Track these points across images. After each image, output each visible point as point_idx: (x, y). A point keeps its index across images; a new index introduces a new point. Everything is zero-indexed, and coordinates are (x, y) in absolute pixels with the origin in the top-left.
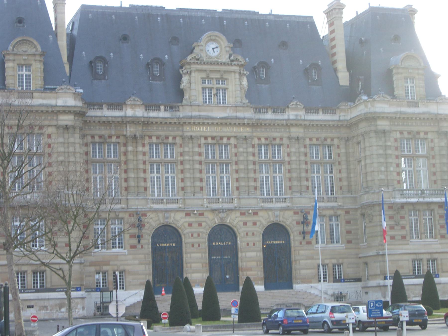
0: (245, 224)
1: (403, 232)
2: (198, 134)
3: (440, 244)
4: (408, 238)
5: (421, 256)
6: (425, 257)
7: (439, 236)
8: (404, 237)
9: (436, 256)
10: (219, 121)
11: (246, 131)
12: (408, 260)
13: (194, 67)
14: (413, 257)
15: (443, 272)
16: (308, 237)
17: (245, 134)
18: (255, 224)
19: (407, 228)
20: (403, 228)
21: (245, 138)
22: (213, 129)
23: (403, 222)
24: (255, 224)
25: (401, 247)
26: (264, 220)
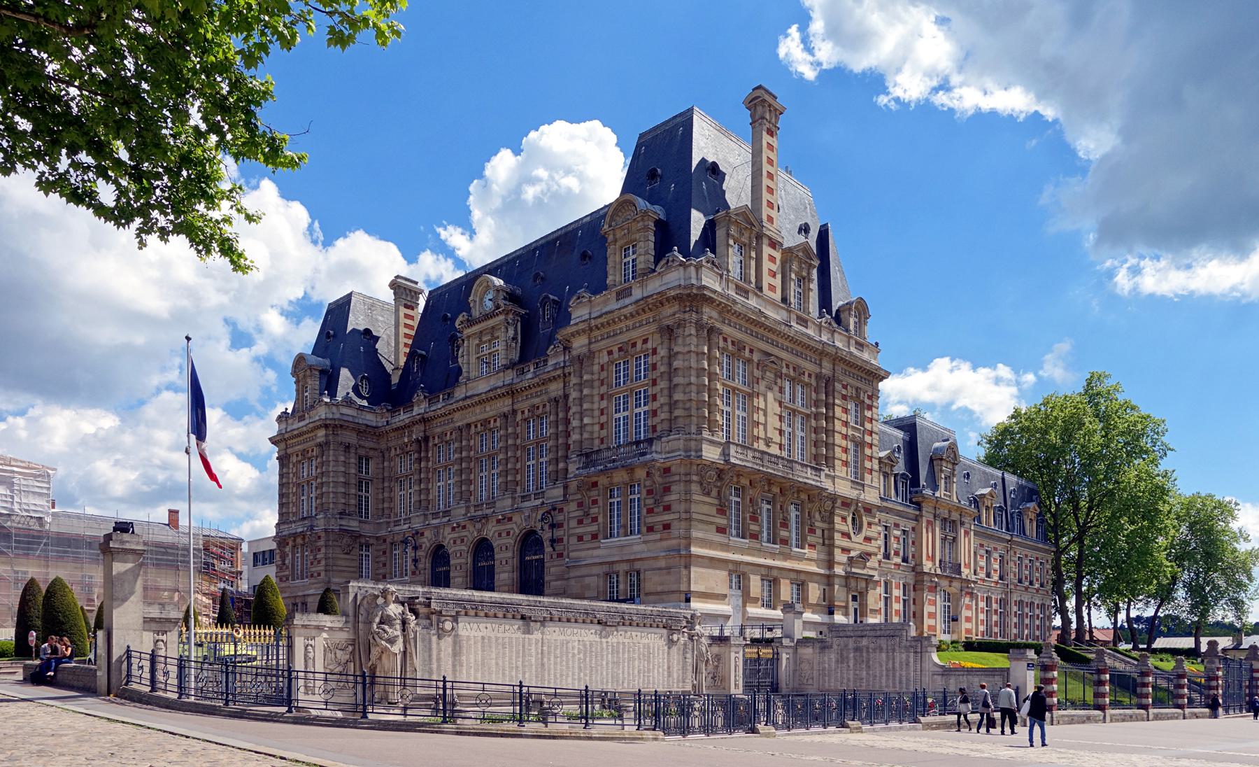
0: (500, 535)
1: (594, 528)
2: (465, 422)
3: (644, 542)
4: (600, 536)
5: (617, 567)
6: (623, 568)
7: (644, 529)
8: (595, 537)
9: (638, 565)
10: (477, 399)
11: (504, 405)
12: (598, 575)
13: (467, 332)
14: (605, 568)
15: (646, 594)
16: (559, 548)
17: (506, 409)
18: (508, 534)
19: (600, 520)
20: (595, 520)
21: (505, 416)
22: (478, 409)
23: (594, 510)
24: (508, 534)
25: (590, 552)
26: (518, 525)
